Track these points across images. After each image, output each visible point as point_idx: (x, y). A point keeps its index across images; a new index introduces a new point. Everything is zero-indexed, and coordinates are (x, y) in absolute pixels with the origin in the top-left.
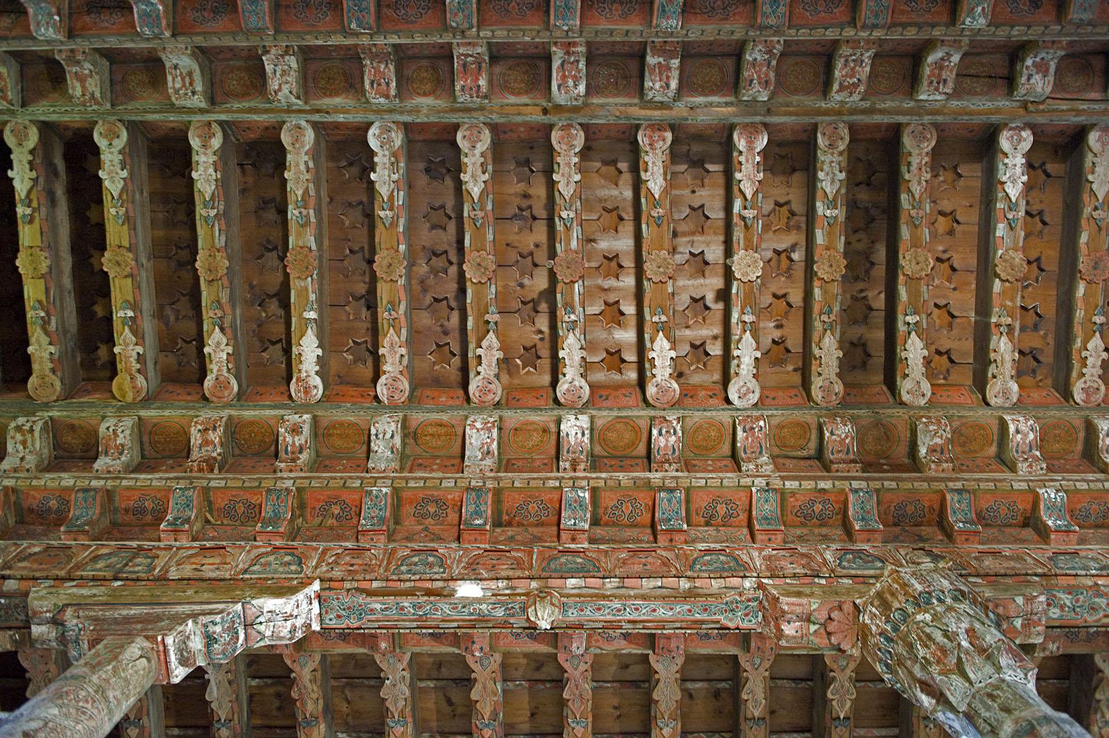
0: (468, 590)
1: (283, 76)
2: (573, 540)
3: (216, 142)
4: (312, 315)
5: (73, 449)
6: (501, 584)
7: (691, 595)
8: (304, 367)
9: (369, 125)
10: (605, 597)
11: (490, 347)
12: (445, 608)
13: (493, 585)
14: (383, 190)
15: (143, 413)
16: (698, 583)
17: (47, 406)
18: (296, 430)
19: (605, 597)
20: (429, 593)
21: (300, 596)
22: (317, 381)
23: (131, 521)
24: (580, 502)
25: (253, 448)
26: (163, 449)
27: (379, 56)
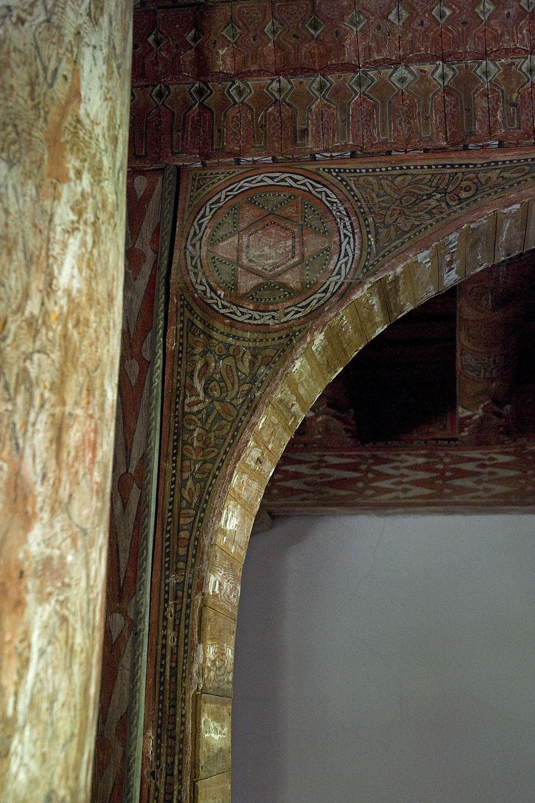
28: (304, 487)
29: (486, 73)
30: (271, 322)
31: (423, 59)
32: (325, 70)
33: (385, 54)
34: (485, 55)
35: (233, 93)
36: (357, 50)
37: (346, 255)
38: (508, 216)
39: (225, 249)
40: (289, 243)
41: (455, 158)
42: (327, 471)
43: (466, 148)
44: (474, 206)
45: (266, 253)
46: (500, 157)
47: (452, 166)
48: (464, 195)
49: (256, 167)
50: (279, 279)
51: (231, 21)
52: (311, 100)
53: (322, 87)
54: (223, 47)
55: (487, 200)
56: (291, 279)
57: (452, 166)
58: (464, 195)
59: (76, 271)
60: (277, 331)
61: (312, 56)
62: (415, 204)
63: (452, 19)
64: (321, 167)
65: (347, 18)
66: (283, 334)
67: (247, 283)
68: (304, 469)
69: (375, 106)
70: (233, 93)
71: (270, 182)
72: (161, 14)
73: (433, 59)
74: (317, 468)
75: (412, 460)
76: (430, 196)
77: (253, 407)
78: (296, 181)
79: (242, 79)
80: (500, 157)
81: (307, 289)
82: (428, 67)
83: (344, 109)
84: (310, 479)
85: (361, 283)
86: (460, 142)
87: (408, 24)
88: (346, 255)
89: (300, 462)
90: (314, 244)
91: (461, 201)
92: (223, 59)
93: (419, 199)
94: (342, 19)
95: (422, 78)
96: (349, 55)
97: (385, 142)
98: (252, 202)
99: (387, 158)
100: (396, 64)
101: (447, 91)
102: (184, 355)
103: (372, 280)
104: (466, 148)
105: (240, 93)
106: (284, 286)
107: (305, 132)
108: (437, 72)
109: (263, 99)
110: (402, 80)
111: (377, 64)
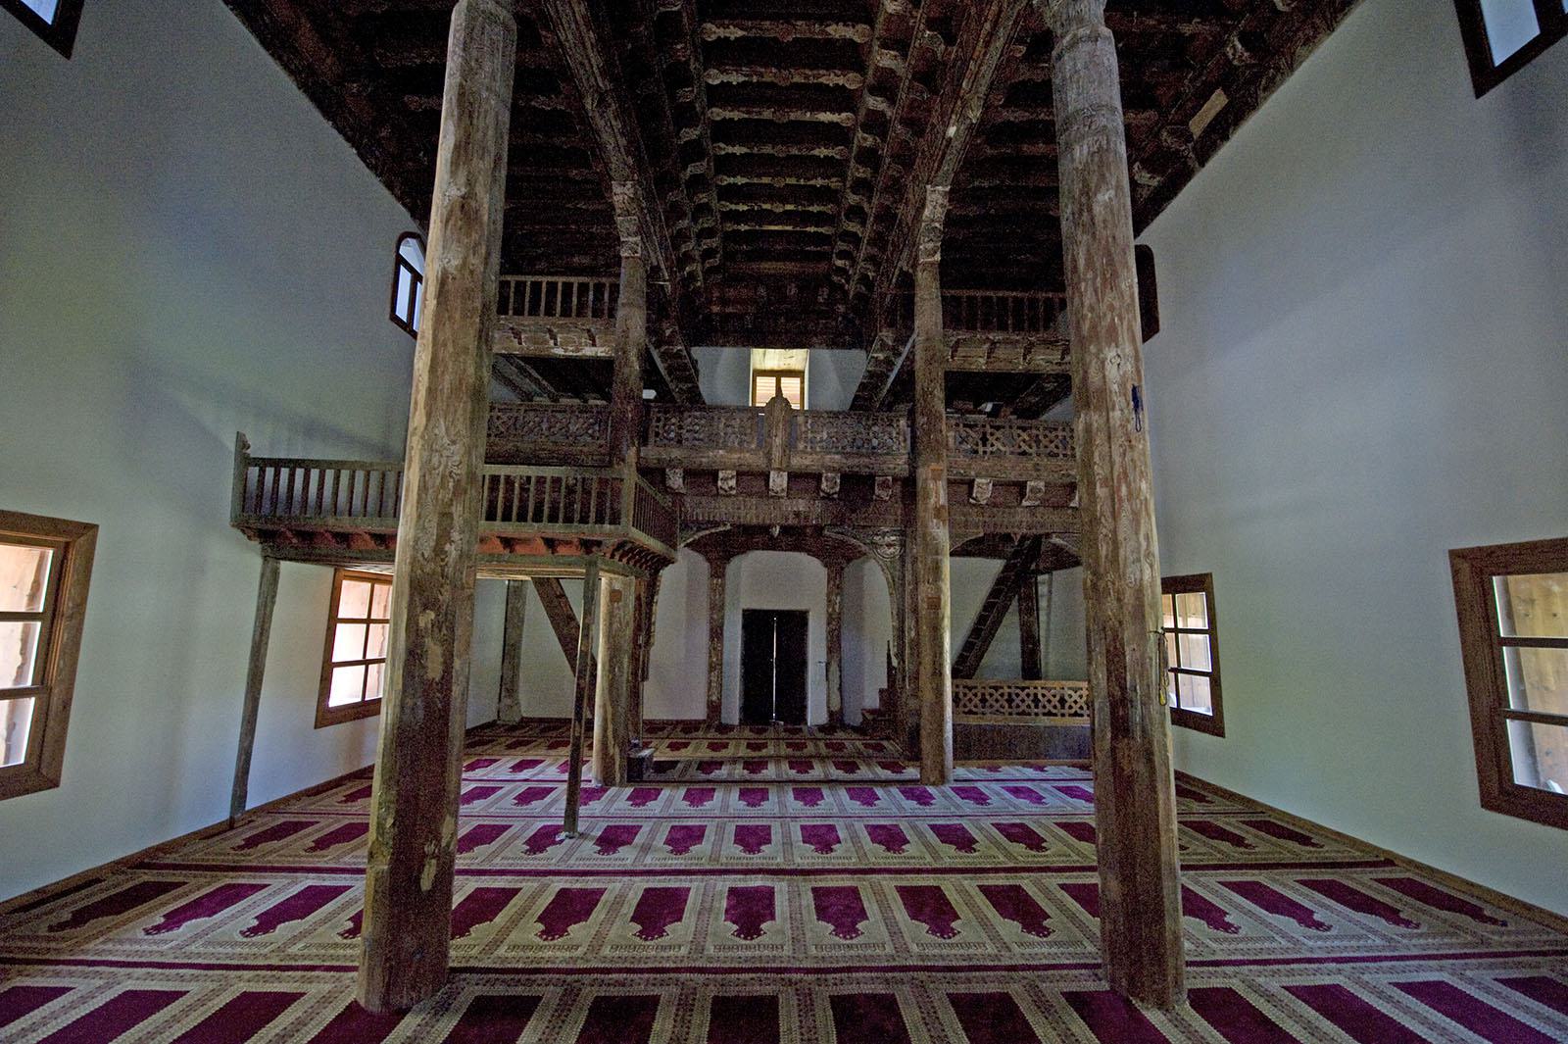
0: (952, 131)
1: (690, 134)
2: (950, 54)
3: (722, 145)
4: (808, 114)
5: (856, 213)
6: (954, 117)
7: (995, 24)
8: (835, 120)
9: (708, 84)
10: (978, 73)
11: (835, 31)
12: (955, 144)
13: (952, 121)
14: (742, 79)
15: (848, 185)
16: (990, 17)
17: (839, 213)
18: (865, 139)
19: (978, 73)
20: (947, 146)
21: (929, 198)
22: (844, 115)
23: (887, 217)
24: (931, 37)
25: (869, 157)
26: (863, 186)
27: (673, 97)
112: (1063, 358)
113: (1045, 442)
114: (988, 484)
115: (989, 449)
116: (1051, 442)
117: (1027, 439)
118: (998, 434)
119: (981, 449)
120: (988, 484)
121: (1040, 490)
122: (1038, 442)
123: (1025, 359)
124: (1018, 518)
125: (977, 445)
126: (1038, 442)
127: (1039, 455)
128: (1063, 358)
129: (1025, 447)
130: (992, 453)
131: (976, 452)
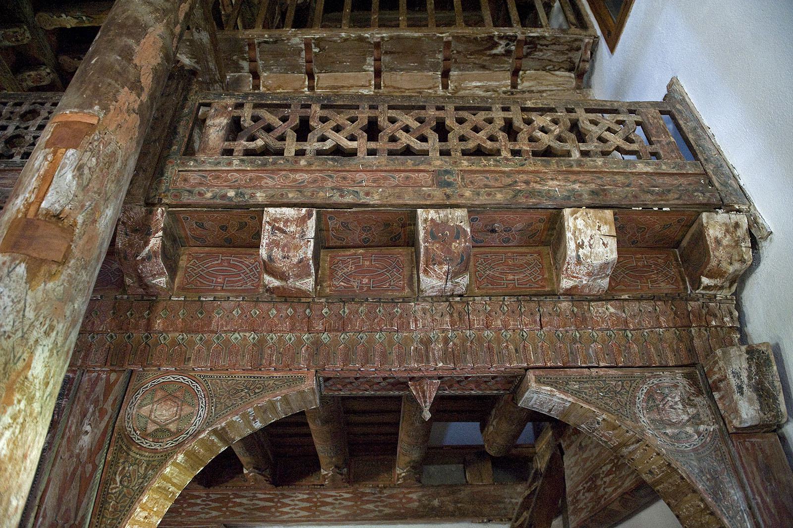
28: (244, 511)
29: (272, 339)
30: (159, 448)
31: (245, 331)
32: (203, 332)
33: (229, 328)
34: (271, 331)
35: (162, 338)
36: (218, 325)
37: (200, 416)
38: (277, 401)
39: (145, 410)
40: (175, 409)
41: (256, 374)
42: (257, 502)
43: (260, 370)
44: (261, 396)
45: (164, 413)
46: (275, 375)
47: (254, 377)
48: (257, 391)
49: (167, 372)
50: (167, 427)
51: (165, 308)
52: (195, 344)
53: (201, 339)
54: (159, 319)
55: (267, 394)
56: (173, 427)
57: (254, 377)
58: (257, 391)
59: (6, 446)
60: (161, 452)
61: (198, 325)
62: (235, 393)
63: (258, 316)
64: (197, 374)
65: (215, 311)
66: (163, 454)
67: (151, 428)
68: (244, 501)
69: (222, 349)
70: (162, 338)
71: (173, 379)
72: (135, 303)
73: (249, 331)
74: (251, 500)
75: (301, 496)
76: (242, 390)
77: (142, 491)
78: (184, 379)
79: (167, 334)
80: (275, 375)
81: (179, 432)
82: (247, 334)
83: (208, 350)
84: (246, 507)
85: (204, 430)
86: (257, 367)
87: (240, 317)
88: (200, 416)
89: (243, 497)
90: (187, 410)
91: (255, 393)
92: (158, 324)
93: (237, 391)
94: (213, 312)
95: (245, 338)
96: (213, 326)
97: (224, 366)
98: (162, 389)
99: (227, 372)
100: (235, 331)
101: (254, 345)
102: (114, 463)
103: (210, 429)
104: (260, 370)
105: (165, 339)
106: (169, 430)
107: (189, 358)
108: (251, 336)
109: (174, 343)
110: (236, 338)
111: (225, 331)
112: (514, 85)
113: (458, 130)
114: (303, 221)
115: (312, 145)
116: (476, 129)
117: (415, 125)
118: (341, 119)
119: (291, 146)
120: (303, 221)
121: (458, 233)
122: (442, 131)
123: (445, 87)
124: (417, 329)
125: (282, 138)
126: (442, 131)
127: (445, 153)
128: (514, 85)
129: (405, 139)
130: (319, 153)
131: (280, 152)
